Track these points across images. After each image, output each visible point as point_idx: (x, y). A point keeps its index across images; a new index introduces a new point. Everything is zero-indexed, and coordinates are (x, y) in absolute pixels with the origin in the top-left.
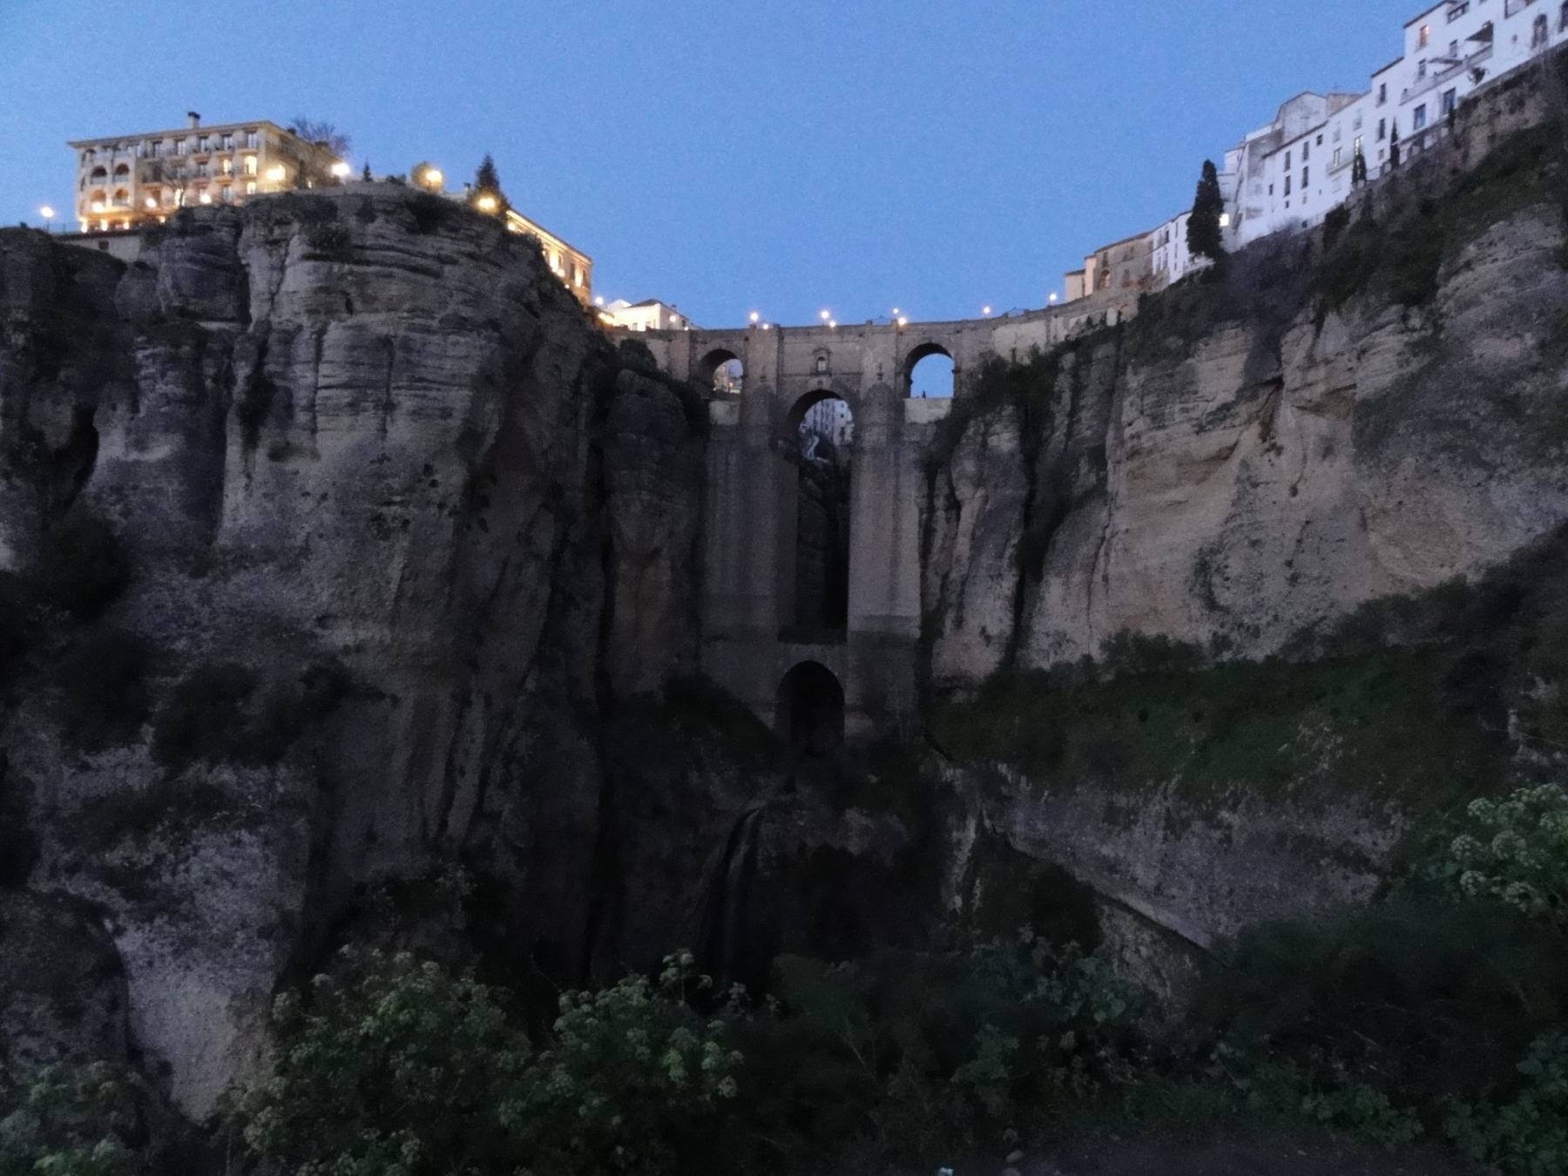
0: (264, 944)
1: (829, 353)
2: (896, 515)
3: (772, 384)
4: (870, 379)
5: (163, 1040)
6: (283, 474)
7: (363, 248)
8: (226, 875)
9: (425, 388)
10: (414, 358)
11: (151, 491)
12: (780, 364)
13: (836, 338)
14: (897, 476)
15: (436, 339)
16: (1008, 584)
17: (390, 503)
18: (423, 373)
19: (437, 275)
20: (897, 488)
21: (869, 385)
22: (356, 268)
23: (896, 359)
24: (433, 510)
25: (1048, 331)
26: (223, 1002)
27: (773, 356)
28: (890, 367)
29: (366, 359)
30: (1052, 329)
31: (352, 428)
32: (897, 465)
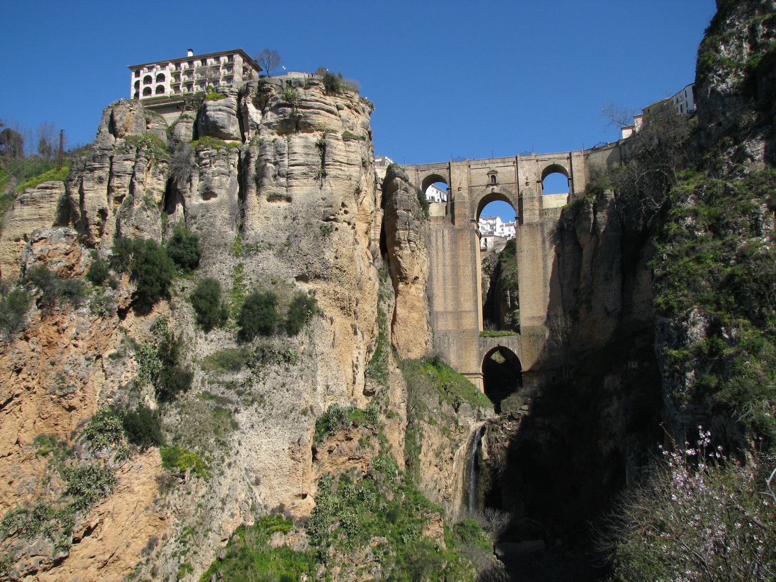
0: (304, 418)
1: (497, 172)
7: (306, 100)
9: (340, 165)
10: (334, 151)
12: (470, 181)
16: (616, 284)
17: (327, 220)
19: (336, 115)
23: (535, 174)
24: (345, 224)
25: (620, 152)
27: (465, 176)
28: (533, 178)
29: (311, 152)
30: (623, 152)
31: (306, 185)
32: (542, 231)
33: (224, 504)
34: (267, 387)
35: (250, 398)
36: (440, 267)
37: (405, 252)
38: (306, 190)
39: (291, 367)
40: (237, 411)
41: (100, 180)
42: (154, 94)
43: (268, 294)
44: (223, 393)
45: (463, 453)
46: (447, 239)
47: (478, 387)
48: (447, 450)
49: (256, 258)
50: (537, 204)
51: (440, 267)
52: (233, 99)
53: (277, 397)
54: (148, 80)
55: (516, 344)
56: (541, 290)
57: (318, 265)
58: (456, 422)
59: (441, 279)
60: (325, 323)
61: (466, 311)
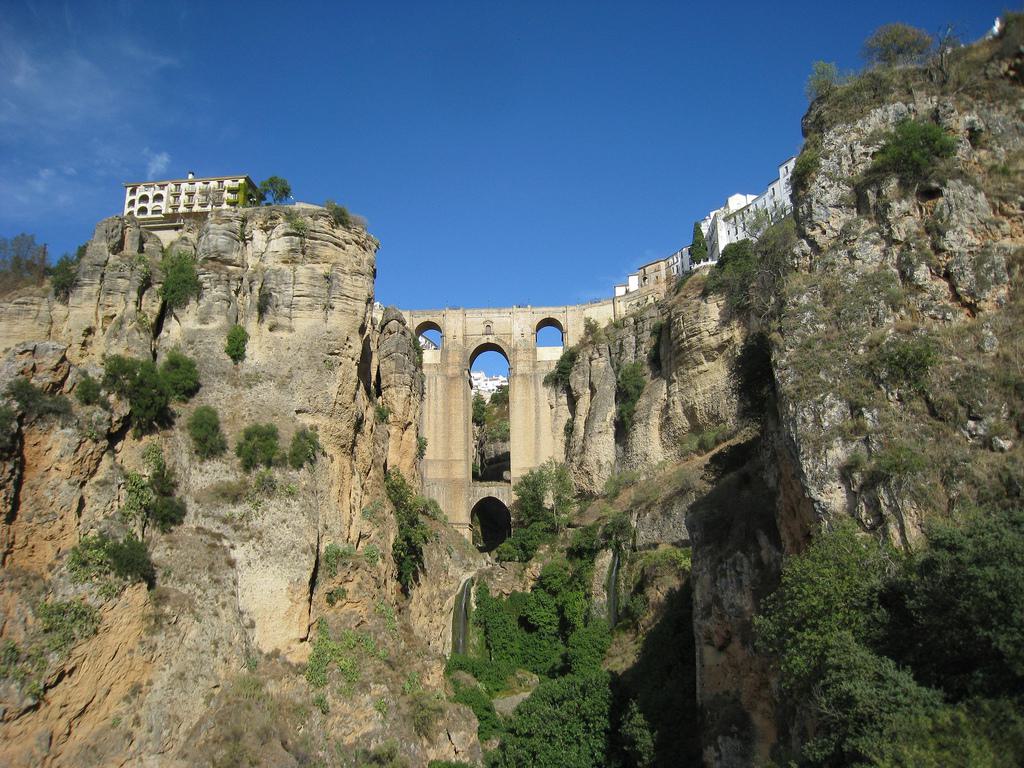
0: (304, 557)
2: (537, 411)
3: (460, 340)
4: (517, 337)
5: (253, 607)
6: (275, 338)
7: (315, 231)
8: (284, 521)
11: (209, 343)
13: (497, 315)
14: (536, 387)
15: (348, 277)
17: (331, 354)
18: (345, 292)
20: (537, 394)
21: (517, 339)
22: (311, 241)
26: (285, 585)
27: (460, 324)
32: (536, 383)
33: (217, 647)
34: (265, 524)
35: (247, 534)
36: (432, 415)
37: (400, 396)
38: (310, 322)
39: (292, 502)
40: (232, 547)
41: (90, 297)
42: (149, 215)
43: (270, 426)
44: (218, 528)
45: (452, 604)
46: (439, 386)
47: (466, 537)
48: (437, 600)
49: (255, 388)
50: (531, 355)
51: (432, 415)
52: (237, 224)
53: (276, 533)
54: (144, 198)
55: (506, 495)
56: (533, 442)
57: (320, 399)
58: (446, 572)
59: (432, 428)
60: (326, 460)
61: (456, 460)
